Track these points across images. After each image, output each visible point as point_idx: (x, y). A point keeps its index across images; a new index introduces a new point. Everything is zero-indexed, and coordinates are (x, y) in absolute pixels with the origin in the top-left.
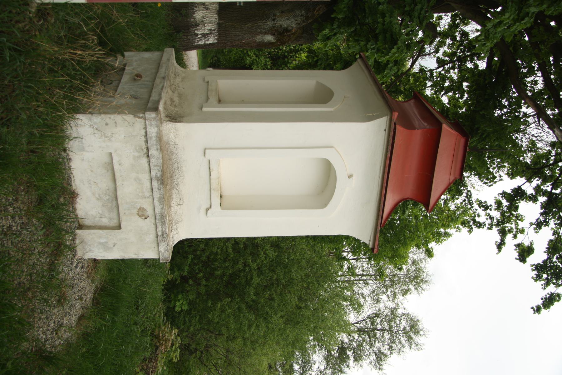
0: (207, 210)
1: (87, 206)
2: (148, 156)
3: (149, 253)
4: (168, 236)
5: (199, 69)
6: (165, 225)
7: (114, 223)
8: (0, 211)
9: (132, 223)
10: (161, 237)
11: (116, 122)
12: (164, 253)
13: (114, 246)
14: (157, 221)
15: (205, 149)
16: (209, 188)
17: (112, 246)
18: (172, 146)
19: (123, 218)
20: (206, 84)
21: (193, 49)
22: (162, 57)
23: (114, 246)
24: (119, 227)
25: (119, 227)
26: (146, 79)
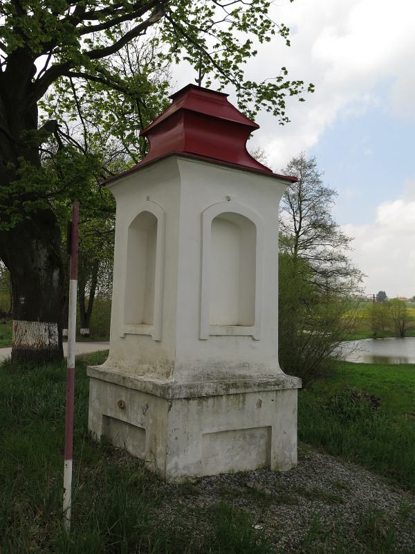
0: (254, 340)
1: (247, 460)
2: (188, 399)
3: (291, 400)
4: (278, 380)
5: (108, 344)
6: (269, 382)
7: (264, 432)
8: (302, 553)
9: (266, 415)
10: (279, 387)
11: (175, 429)
12: (296, 382)
13: (285, 433)
14: (266, 390)
15: (200, 339)
16: (215, 337)
17: (285, 436)
18: (196, 373)
19: (262, 424)
20: (128, 336)
21: (411, 364)
22: (93, 378)
23: (285, 433)
24: (269, 428)
25: (269, 428)
26: (124, 396)
